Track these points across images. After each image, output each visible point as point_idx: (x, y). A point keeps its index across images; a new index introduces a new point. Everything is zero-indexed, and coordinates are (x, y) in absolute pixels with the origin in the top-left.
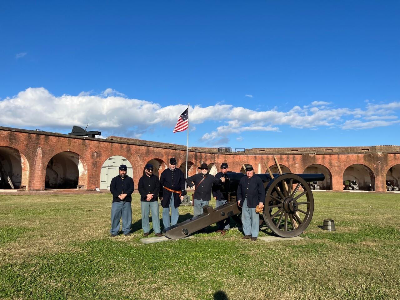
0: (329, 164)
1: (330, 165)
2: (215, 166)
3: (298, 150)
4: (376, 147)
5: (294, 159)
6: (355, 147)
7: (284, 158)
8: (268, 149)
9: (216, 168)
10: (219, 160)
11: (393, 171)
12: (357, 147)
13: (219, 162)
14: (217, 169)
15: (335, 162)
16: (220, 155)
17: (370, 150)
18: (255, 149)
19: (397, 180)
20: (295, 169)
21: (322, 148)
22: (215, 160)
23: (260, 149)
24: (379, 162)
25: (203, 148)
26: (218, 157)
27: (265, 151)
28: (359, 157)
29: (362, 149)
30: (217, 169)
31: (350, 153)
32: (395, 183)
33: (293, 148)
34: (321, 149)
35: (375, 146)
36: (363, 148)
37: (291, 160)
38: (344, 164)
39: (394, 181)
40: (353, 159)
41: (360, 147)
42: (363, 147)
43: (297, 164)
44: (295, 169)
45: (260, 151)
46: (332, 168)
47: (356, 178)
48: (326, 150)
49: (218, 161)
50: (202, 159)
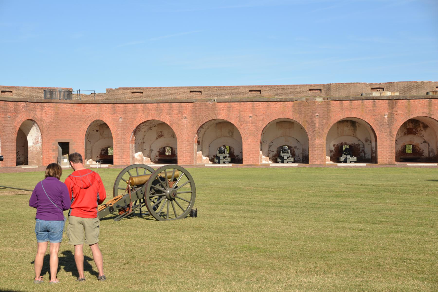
0: (238, 119)
1: (240, 121)
2: (36, 125)
3: (201, 92)
4: (332, 86)
5: (180, 112)
6: (299, 85)
7: (162, 108)
8: (147, 90)
9: (38, 128)
10: (43, 112)
11: (358, 128)
12: (302, 85)
13: (44, 117)
14: (40, 130)
15: (247, 115)
16: (45, 104)
17: (322, 91)
18: (124, 89)
19: (364, 145)
20: (182, 129)
21: (242, 87)
22: (35, 114)
23: (133, 88)
24: (316, 114)
25: (19, 87)
26: (42, 108)
27: (142, 93)
28: (285, 106)
29: (310, 90)
30: (39, 131)
31: (271, 100)
32: (361, 149)
33: (192, 87)
34: (242, 89)
35: (330, 84)
36: (312, 88)
37: (175, 112)
38: (262, 119)
39: (359, 145)
40: (286, 111)
41: (307, 85)
42: (311, 85)
43: (185, 120)
44: (182, 129)
45: (133, 93)
46: (242, 126)
47: (298, 141)
48: (250, 91)
49: (43, 116)
50: (9, 112)
